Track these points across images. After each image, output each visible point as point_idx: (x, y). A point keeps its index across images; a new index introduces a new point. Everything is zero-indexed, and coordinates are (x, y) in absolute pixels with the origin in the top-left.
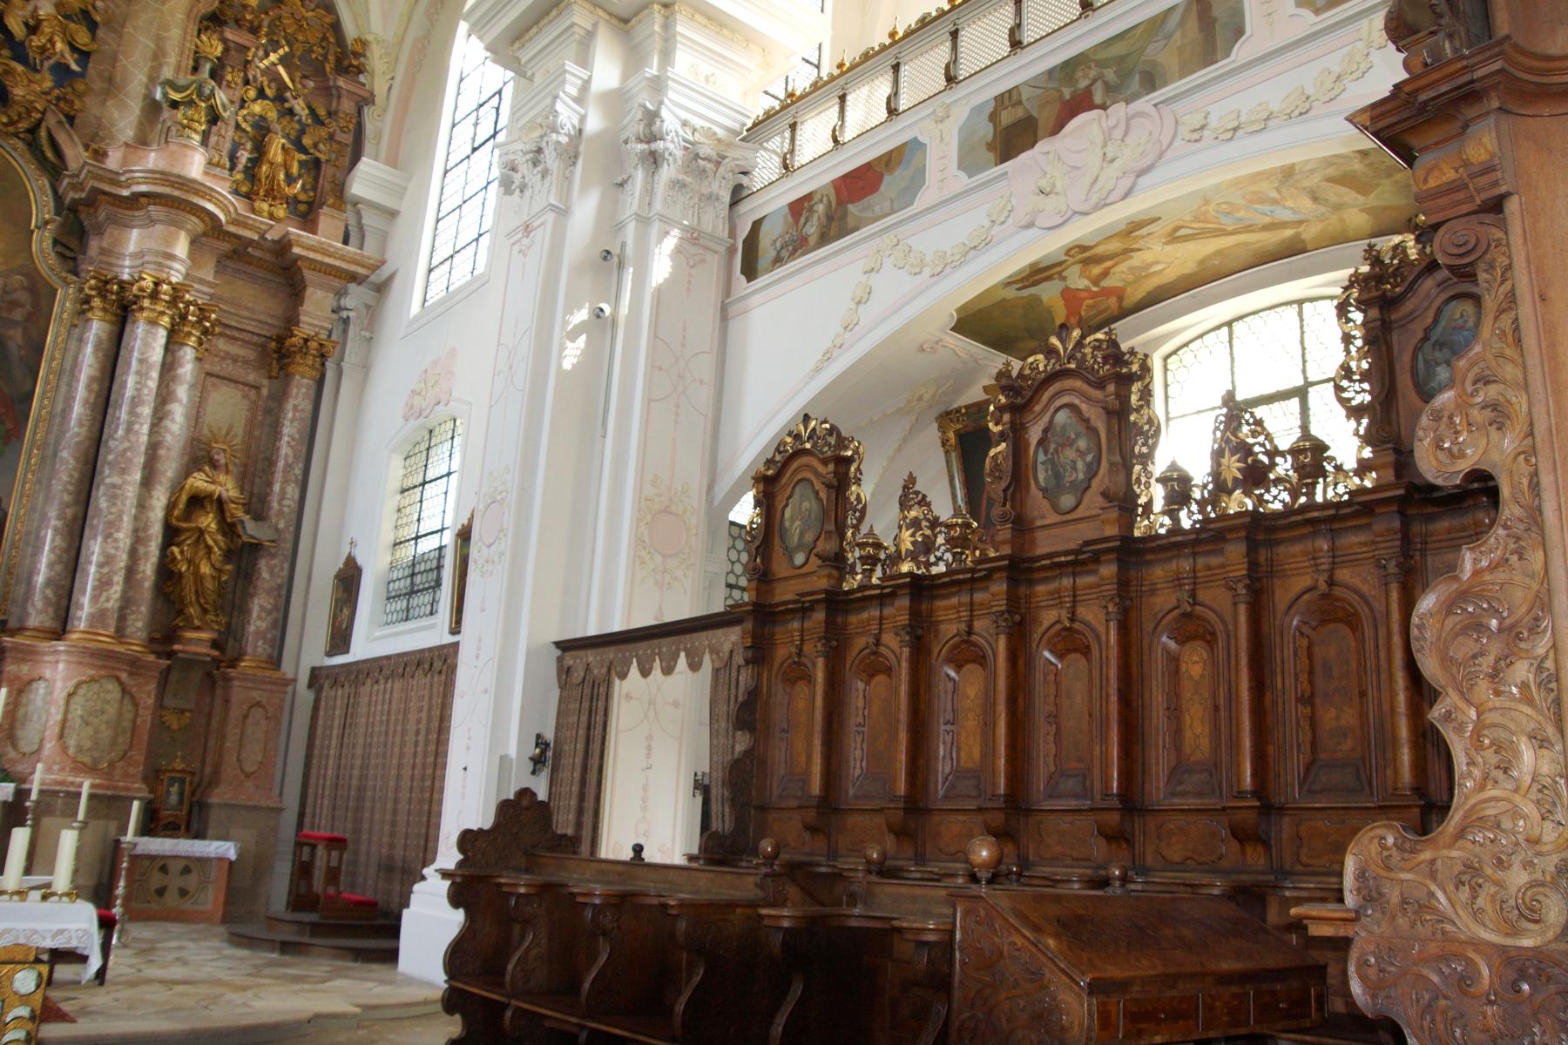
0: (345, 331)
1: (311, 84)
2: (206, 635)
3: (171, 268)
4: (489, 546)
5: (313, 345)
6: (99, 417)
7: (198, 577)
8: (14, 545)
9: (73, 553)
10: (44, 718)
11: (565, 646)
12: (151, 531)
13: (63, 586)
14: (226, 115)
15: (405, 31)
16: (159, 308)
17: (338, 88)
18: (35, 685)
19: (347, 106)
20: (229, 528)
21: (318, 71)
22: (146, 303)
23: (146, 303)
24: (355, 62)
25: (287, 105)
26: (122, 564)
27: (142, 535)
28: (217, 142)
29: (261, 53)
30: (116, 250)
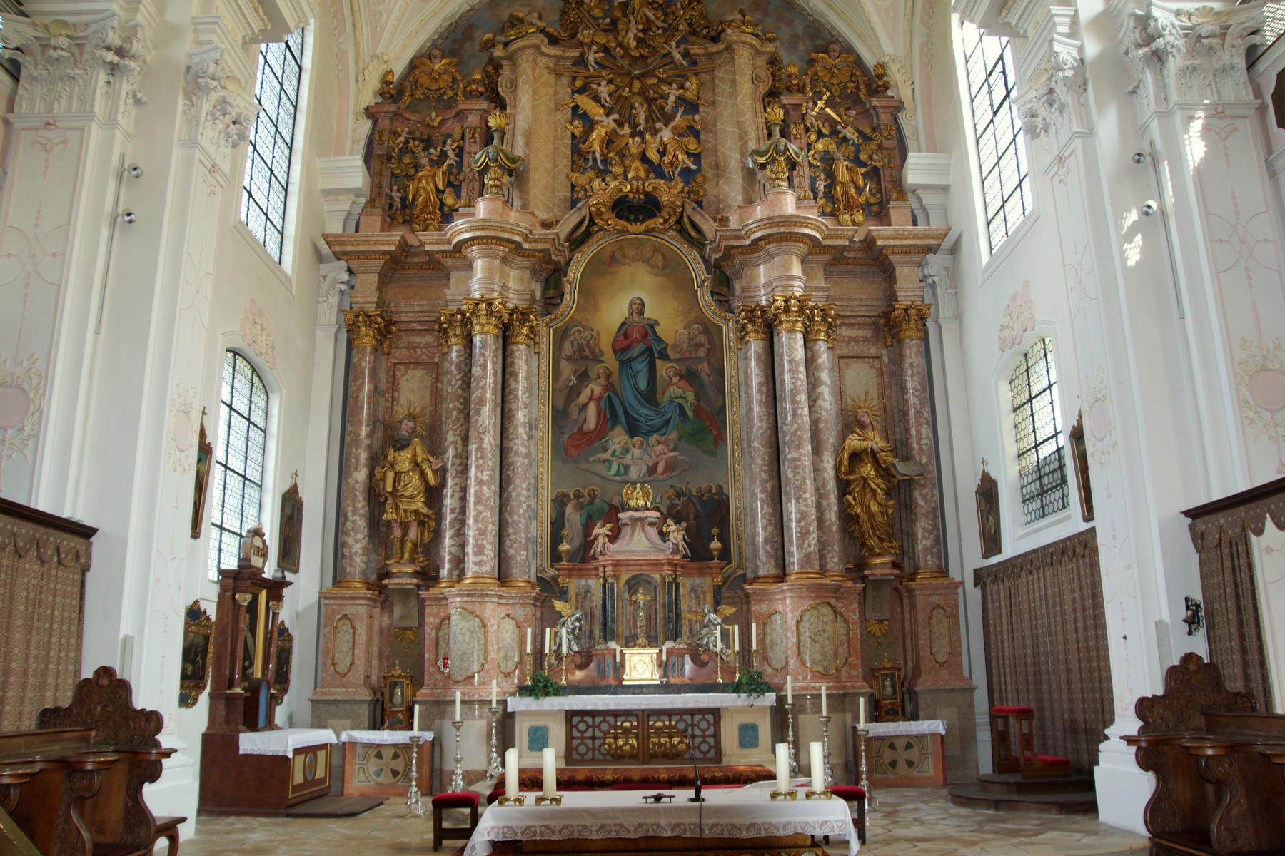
0: (934, 294)
1: (854, 112)
2: (886, 559)
3: (793, 286)
4: (1102, 440)
5: (913, 312)
6: (772, 411)
7: (870, 515)
8: (738, 519)
9: (778, 516)
10: (784, 640)
11: (1194, 514)
12: (828, 488)
13: (776, 542)
14: (800, 160)
15: (911, 43)
16: (793, 318)
17: (874, 108)
18: (774, 618)
19: (885, 118)
20: (885, 472)
21: (856, 100)
22: (783, 317)
23: (783, 317)
24: (880, 83)
25: (840, 135)
26: (814, 517)
27: (822, 491)
28: (800, 183)
29: (811, 104)
30: (753, 285)
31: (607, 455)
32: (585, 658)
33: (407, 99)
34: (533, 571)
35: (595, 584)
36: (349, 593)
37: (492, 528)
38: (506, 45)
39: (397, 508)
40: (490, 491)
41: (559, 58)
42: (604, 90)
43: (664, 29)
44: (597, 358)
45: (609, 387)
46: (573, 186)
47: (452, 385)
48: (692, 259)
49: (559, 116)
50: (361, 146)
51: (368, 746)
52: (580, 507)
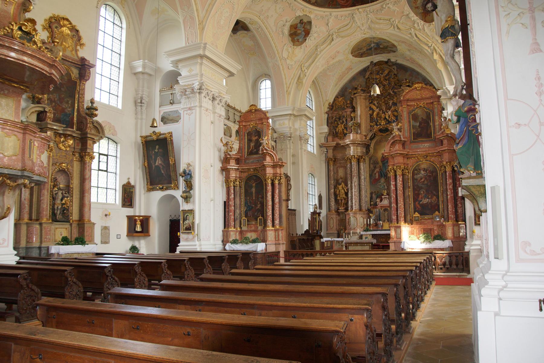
31: (381, 184)
32: (376, 225)
33: (334, 108)
34: (367, 207)
35: (378, 210)
36: (332, 213)
37: (358, 201)
38: (355, 94)
39: (340, 197)
40: (357, 194)
41: (365, 96)
42: (376, 103)
43: (389, 85)
44: (378, 163)
45: (381, 169)
46: (371, 126)
47: (349, 172)
49: (367, 109)
50: (326, 120)
51: (337, 241)
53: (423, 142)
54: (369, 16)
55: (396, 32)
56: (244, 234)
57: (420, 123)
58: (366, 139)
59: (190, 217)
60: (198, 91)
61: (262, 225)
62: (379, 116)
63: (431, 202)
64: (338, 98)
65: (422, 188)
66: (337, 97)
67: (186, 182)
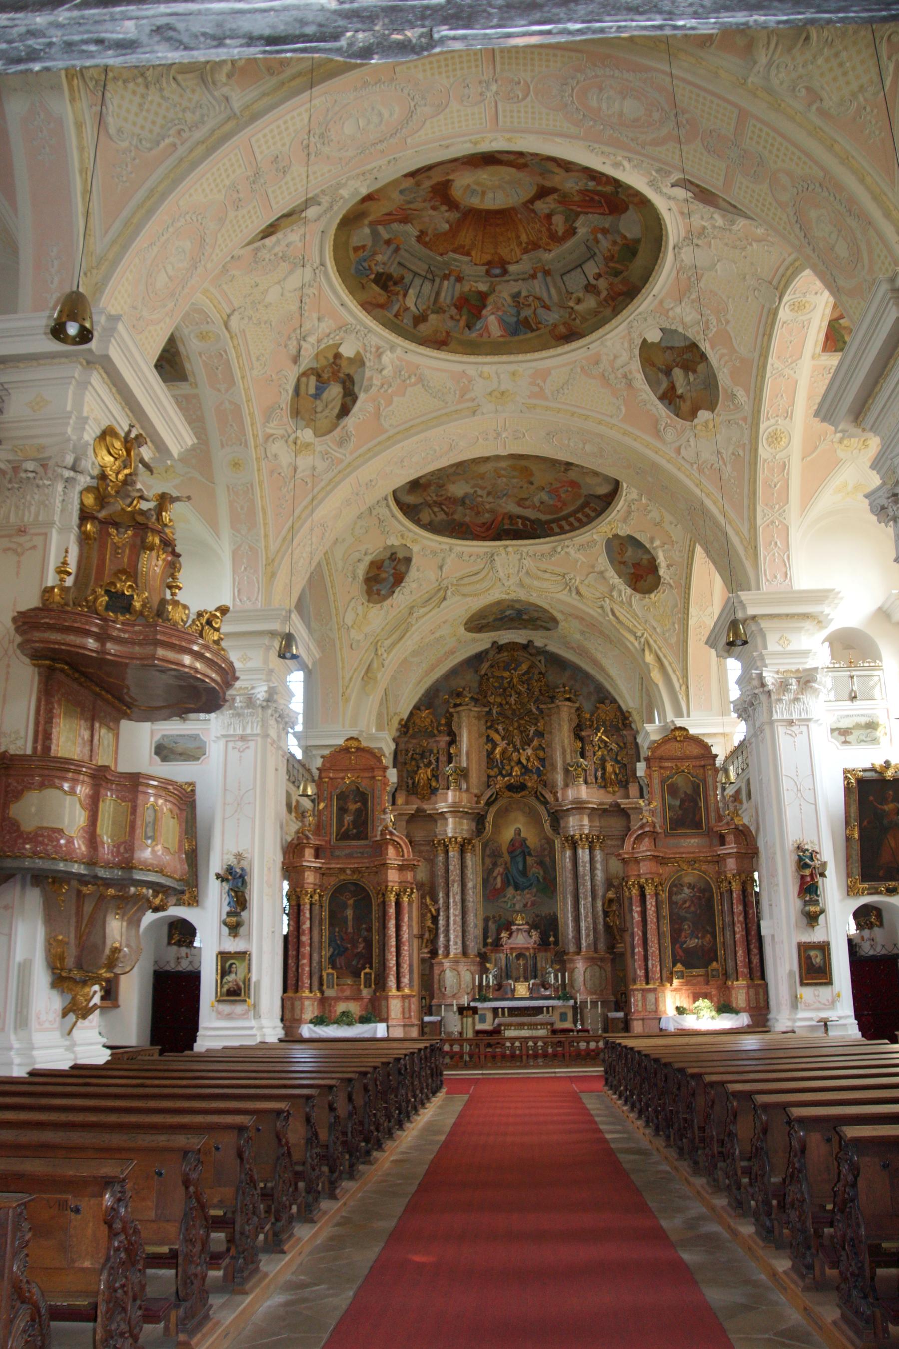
19: (630, 739)
21: (618, 730)
32: (499, 987)
33: (411, 732)
35: (503, 956)
38: (456, 706)
40: (459, 919)
44: (501, 856)
45: (506, 869)
46: (489, 777)
47: (440, 872)
48: (542, 810)
52: (495, 922)
53: (686, 836)
54: (525, 562)
55: (573, 599)
56: (330, 1005)
57: (682, 802)
58: (478, 803)
59: (240, 968)
60: (264, 704)
61: (370, 986)
62: (507, 755)
63: (703, 946)
64: (419, 709)
65: (683, 919)
66: (417, 708)
67: (236, 892)
